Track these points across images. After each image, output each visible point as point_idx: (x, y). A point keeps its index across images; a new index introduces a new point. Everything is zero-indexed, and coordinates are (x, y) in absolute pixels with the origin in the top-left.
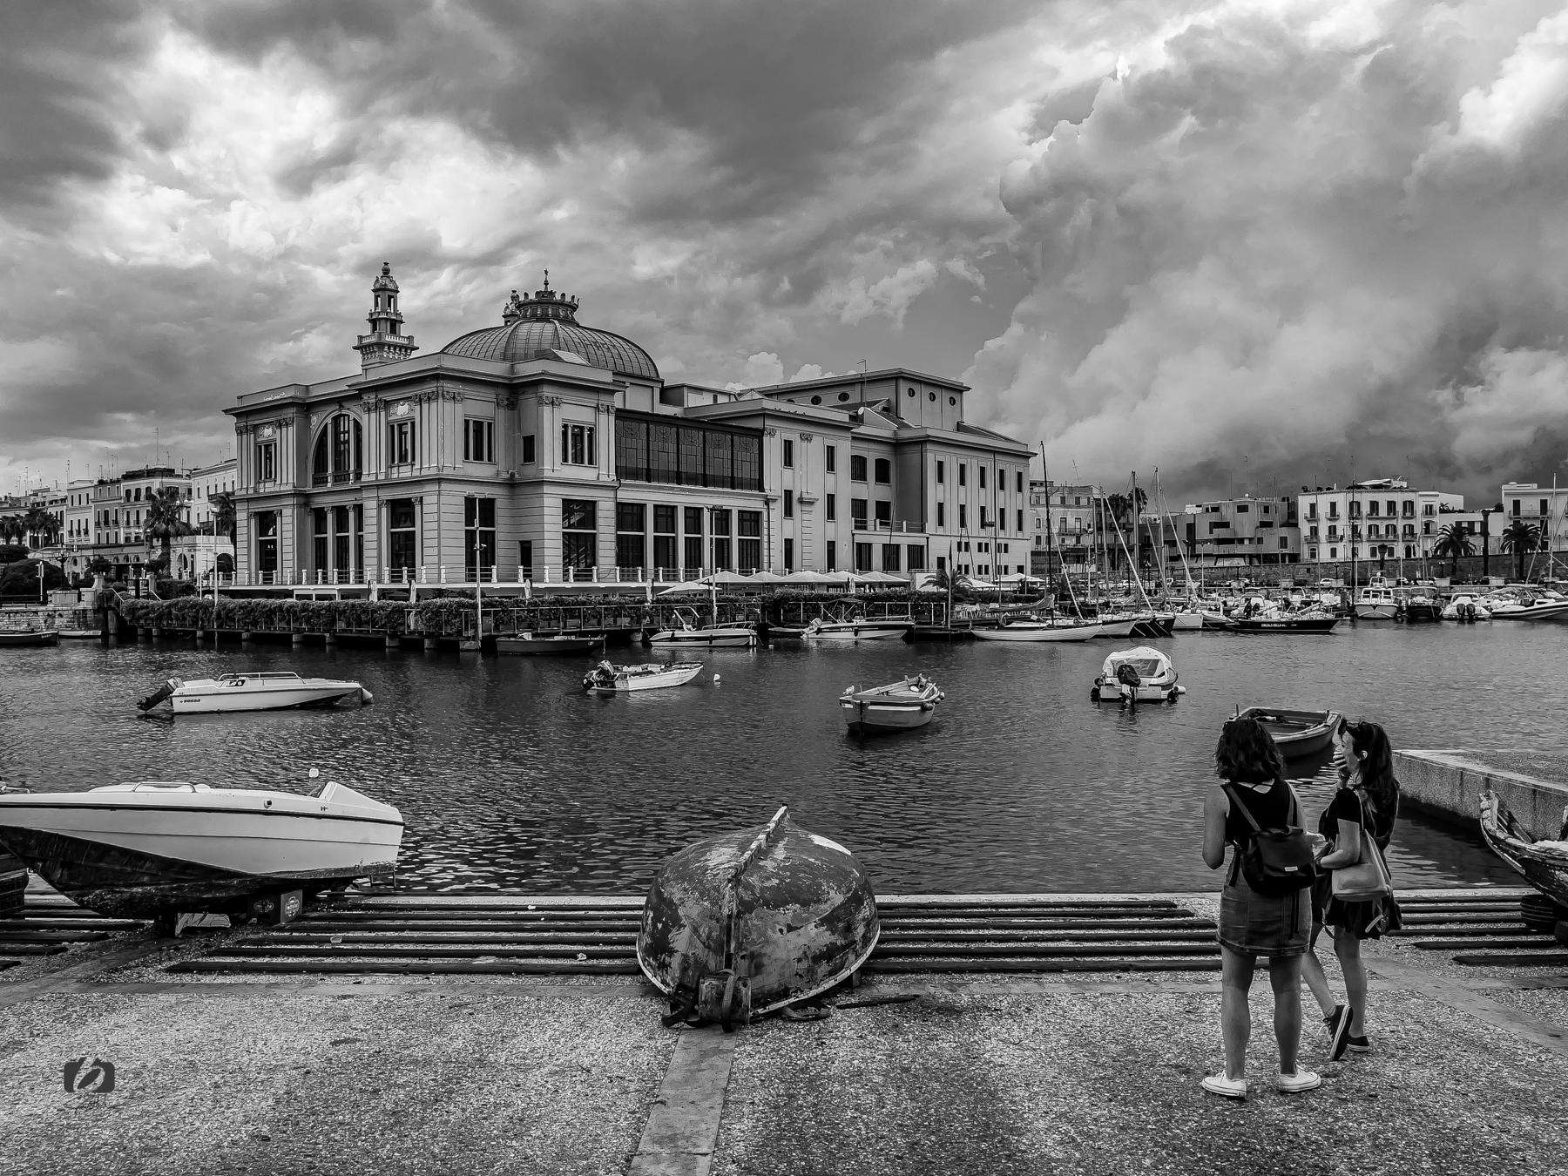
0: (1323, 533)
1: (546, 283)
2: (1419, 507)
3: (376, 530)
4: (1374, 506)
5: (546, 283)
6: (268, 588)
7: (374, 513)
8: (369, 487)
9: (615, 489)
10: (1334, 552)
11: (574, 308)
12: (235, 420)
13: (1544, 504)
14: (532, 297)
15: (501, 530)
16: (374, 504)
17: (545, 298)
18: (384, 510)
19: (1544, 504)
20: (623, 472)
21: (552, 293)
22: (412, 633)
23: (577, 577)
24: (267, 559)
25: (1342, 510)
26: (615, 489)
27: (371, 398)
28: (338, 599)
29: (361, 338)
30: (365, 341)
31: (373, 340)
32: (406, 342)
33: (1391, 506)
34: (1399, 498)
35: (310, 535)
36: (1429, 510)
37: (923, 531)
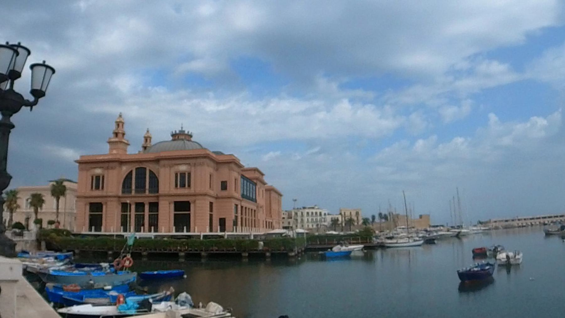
0: (299, 220)
1: (182, 128)
2: (323, 214)
3: (167, 213)
4: (308, 213)
5: (182, 128)
6: (107, 233)
7: (168, 205)
8: (165, 196)
9: (241, 201)
10: (313, 226)
11: (191, 136)
12: (78, 164)
13: (351, 213)
14: (178, 132)
15: (214, 213)
16: (168, 203)
17: (182, 133)
18: (172, 206)
19: (351, 213)
20: (243, 196)
21: (184, 131)
22: (260, 250)
23: (96, 230)
24: (96, 221)
25: (305, 214)
26: (241, 201)
27: (166, 162)
28: (115, 238)
29: (110, 138)
30: (113, 140)
31: (117, 140)
32: (126, 142)
33: (312, 213)
34: (318, 211)
35: (120, 213)
36: (325, 214)
37: (271, 217)
